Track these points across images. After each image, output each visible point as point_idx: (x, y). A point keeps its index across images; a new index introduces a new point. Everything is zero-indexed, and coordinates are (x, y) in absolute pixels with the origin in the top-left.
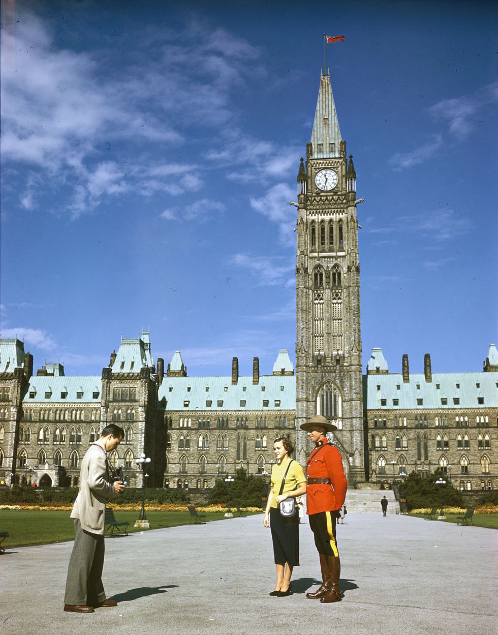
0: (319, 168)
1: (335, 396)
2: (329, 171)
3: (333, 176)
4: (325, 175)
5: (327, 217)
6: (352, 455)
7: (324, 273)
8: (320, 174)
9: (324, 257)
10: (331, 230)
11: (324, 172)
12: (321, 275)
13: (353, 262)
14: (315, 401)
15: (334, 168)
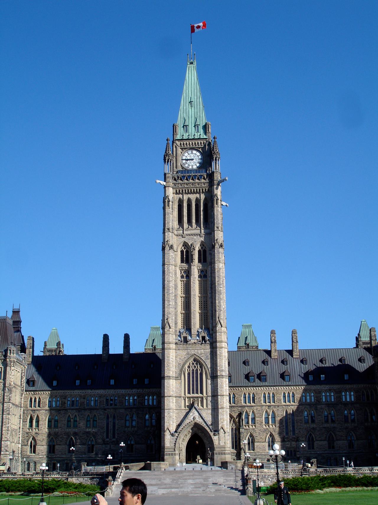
2: (194, 152)
8: (186, 154)
11: (190, 152)
15: (199, 148)
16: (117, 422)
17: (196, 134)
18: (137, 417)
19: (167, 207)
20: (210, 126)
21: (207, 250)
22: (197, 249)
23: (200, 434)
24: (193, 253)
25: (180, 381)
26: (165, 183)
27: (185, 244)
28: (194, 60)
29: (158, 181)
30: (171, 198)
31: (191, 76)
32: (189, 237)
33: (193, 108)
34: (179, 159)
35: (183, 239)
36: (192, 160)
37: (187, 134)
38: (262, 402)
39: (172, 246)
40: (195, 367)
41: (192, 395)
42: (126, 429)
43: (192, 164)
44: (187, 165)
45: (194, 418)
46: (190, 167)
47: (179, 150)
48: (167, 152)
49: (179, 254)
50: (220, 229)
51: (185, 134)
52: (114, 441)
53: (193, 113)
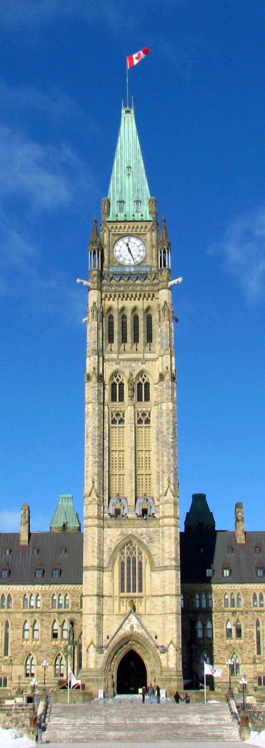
0: (119, 235)
1: (140, 563)
2: (133, 240)
3: (138, 246)
4: (127, 245)
5: (129, 304)
6: (164, 650)
7: (125, 382)
8: (120, 243)
9: (124, 360)
10: (136, 318)
11: (126, 240)
12: (122, 385)
13: (167, 368)
14: (112, 571)
15: (140, 234)
16: (10, 632)
17: (136, 214)
18: (42, 625)
21: (151, 383)
23: (139, 651)
25: (110, 573)
33: (131, 177)
37: (123, 214)
38: (223, 606)
40: (131, 553)
41: (125, 594)
42: (24, 643)
45: (132, 627)
51: (119, 215)
52: (6, 660)
53: (131, 184)
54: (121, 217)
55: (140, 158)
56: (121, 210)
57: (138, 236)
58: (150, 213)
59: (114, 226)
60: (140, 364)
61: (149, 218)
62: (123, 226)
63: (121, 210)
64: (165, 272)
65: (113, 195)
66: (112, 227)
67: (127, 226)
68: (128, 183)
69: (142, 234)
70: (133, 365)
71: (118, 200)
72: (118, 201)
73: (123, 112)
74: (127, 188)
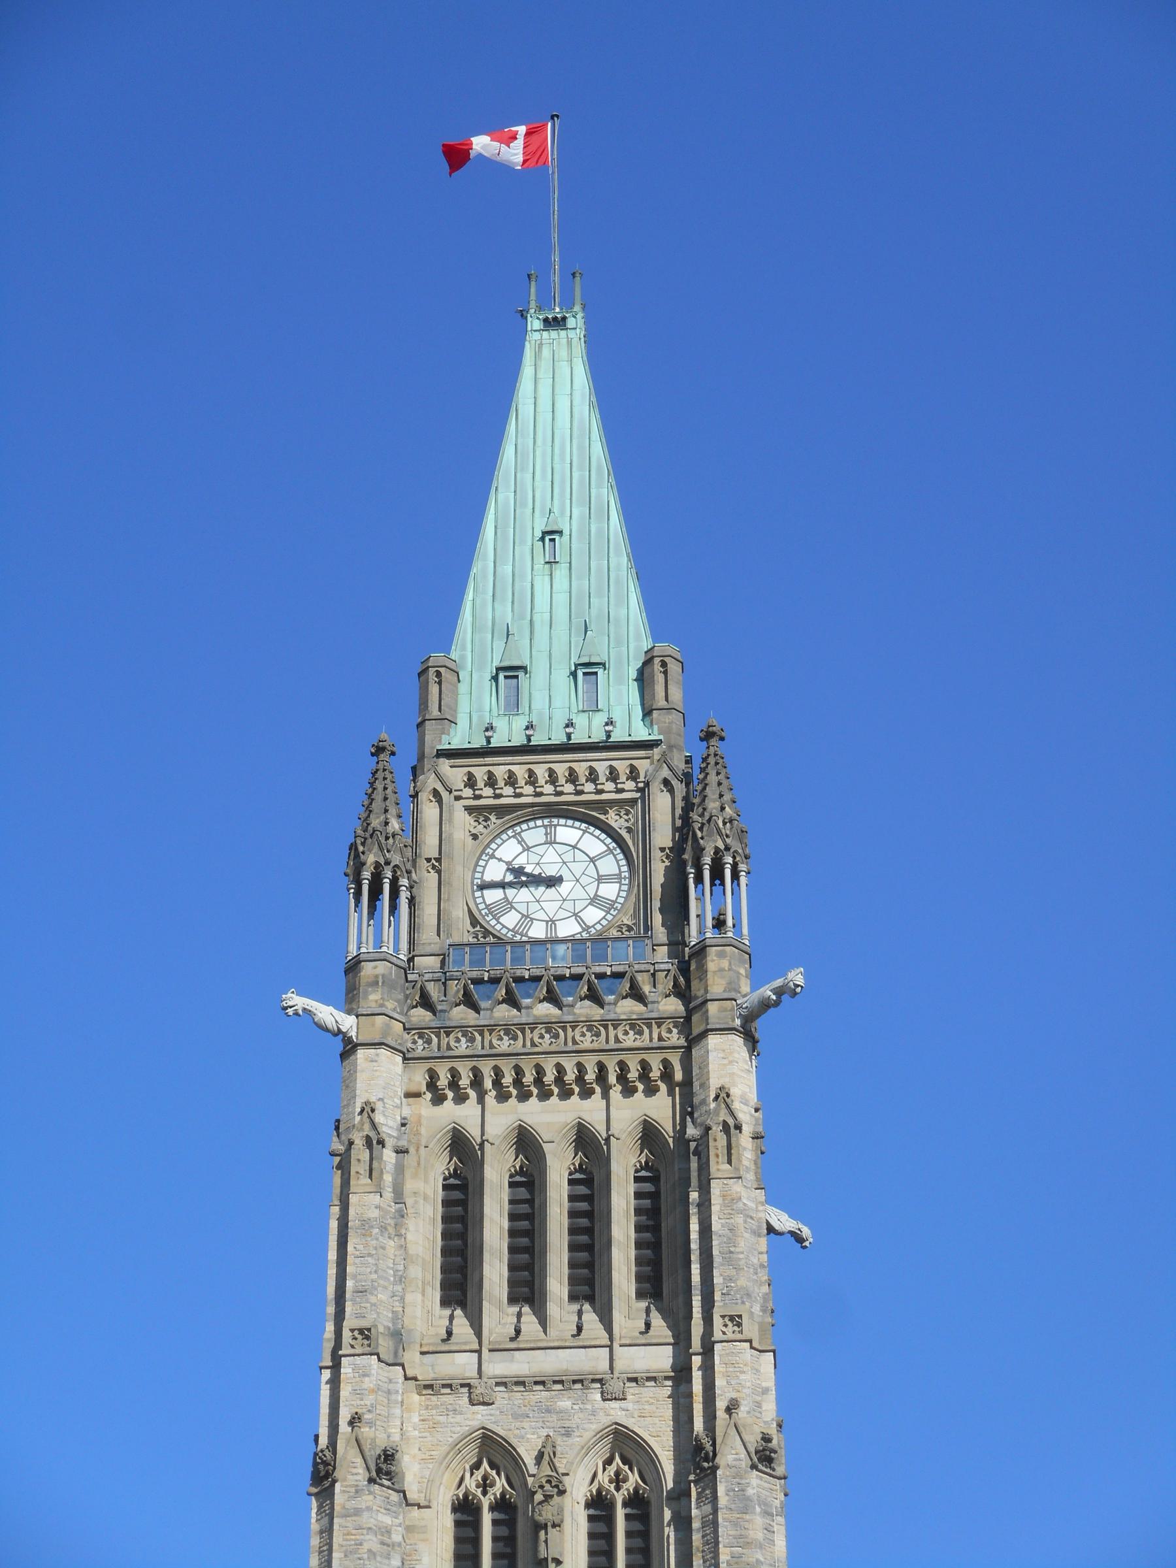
2: (568, 832)
3: (593, 860)
8: (509, 850)
15: (603, 806)
17: (581, 721)
19: (360, 1181)
20: (674, 668)
22: (579, 1490)
24: (546, 1514)
26: (348, 1023)
27: (493, 1450)
28: (568, 304)
29: (297, 1001)
30: (387, 1123)
31: (555, 388)
32: (518, 1397)
33: (561, 572)
34: (459, 873)
35: (480, 1416)
36: (553, 882)
37: (520, 722)
39: (388, 1456)
43: (551, 908)
44: (510, 920)
46: (538, 931)
47: (462, 822)
48: (376, 822)
49: (440, 1527)
50: (750, 1329)
53: (561, 599)
54: (509, 733)
55: (606, 495)
56: (514, 705)
57: (588, 815)
58: (647, 713)
59: (480, 774)
60: (598, 1397)
61: (641, 733)
62: (520, 772)
63: (514, 705)
64: (721, 955)
65: (473, 648)
66: (471, 782)
67: (541, 772)
68: (551, 594)
69: (612, 803)
70: (565, 1403)
71: (496, 663)
72: (498, 669)
73: (535, 323)
74: (541, 618)
